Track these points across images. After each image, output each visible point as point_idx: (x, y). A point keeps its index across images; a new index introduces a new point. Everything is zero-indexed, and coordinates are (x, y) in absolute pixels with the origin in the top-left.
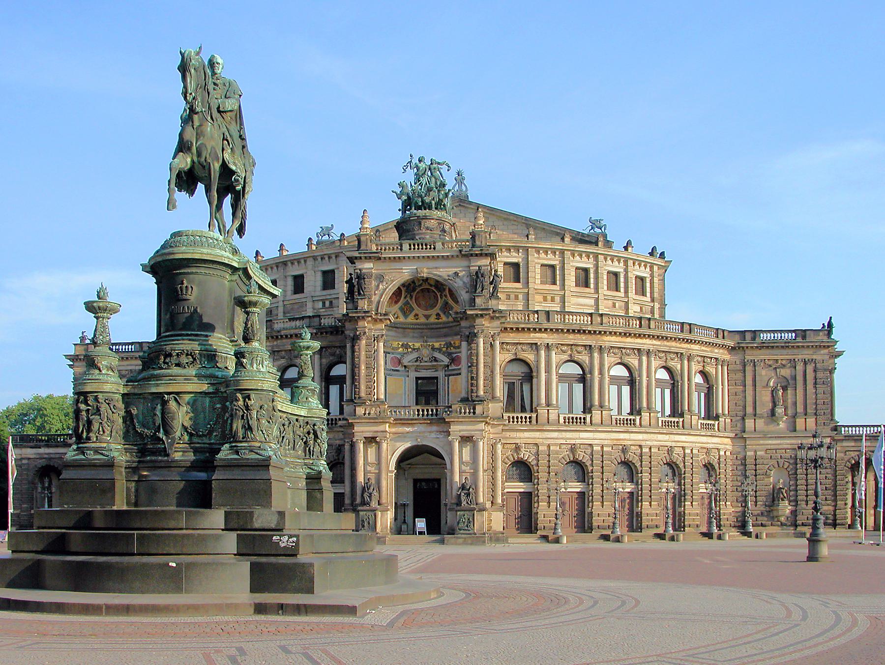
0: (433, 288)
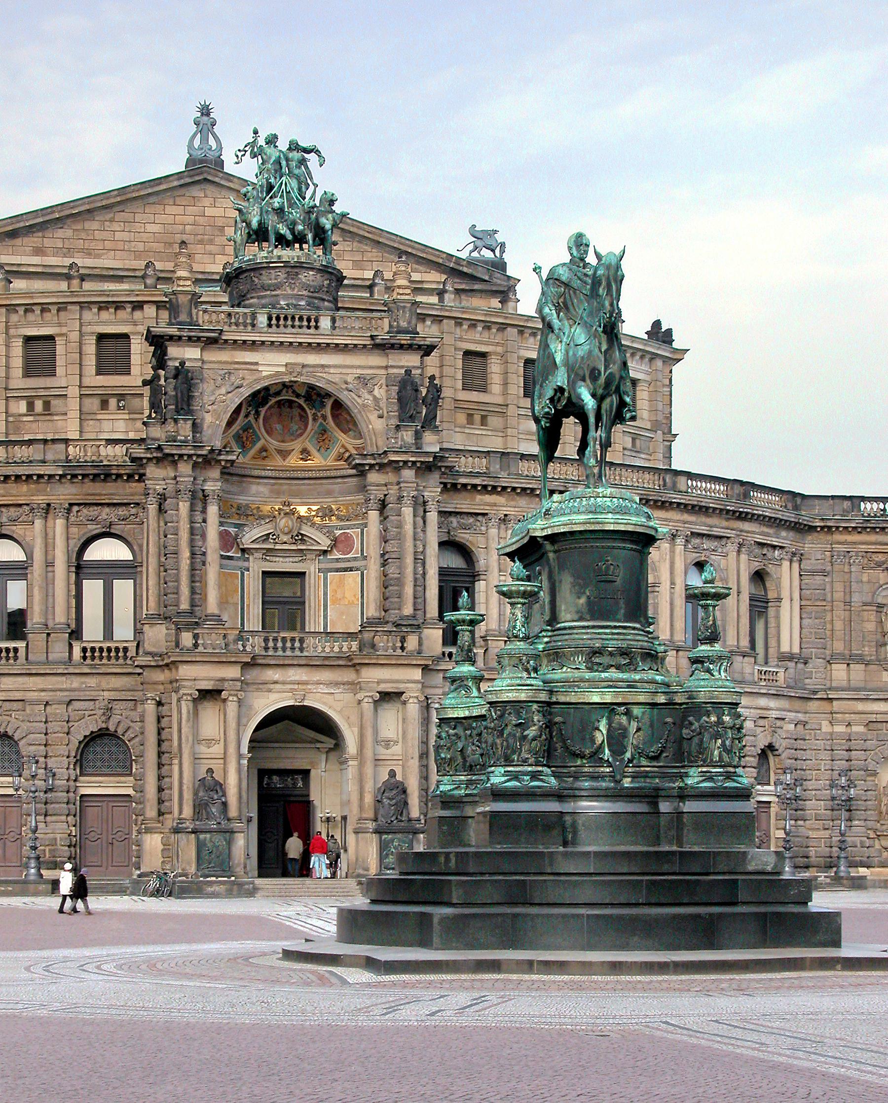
0: (301, 401)
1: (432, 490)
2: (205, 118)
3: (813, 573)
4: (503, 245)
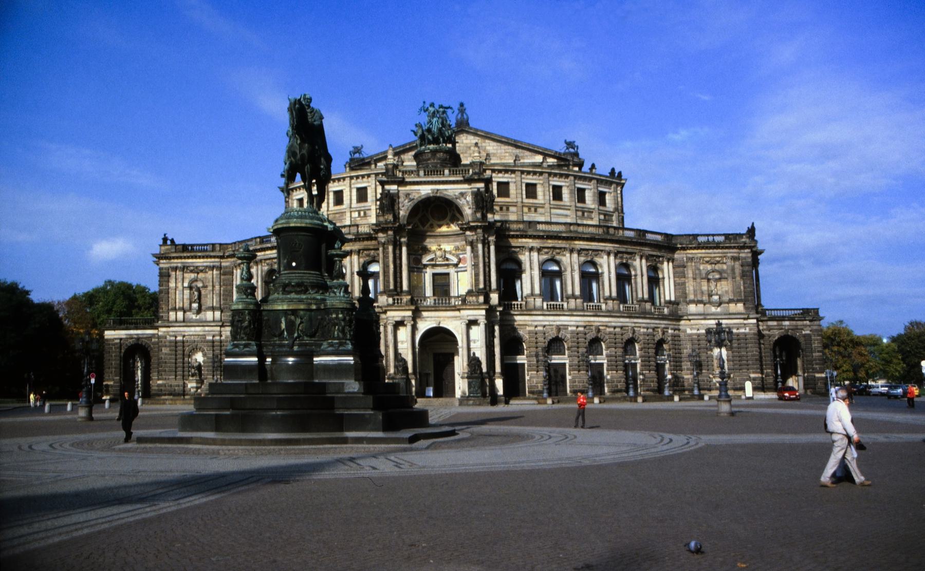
2: (462, 108)
3: (679, 267)
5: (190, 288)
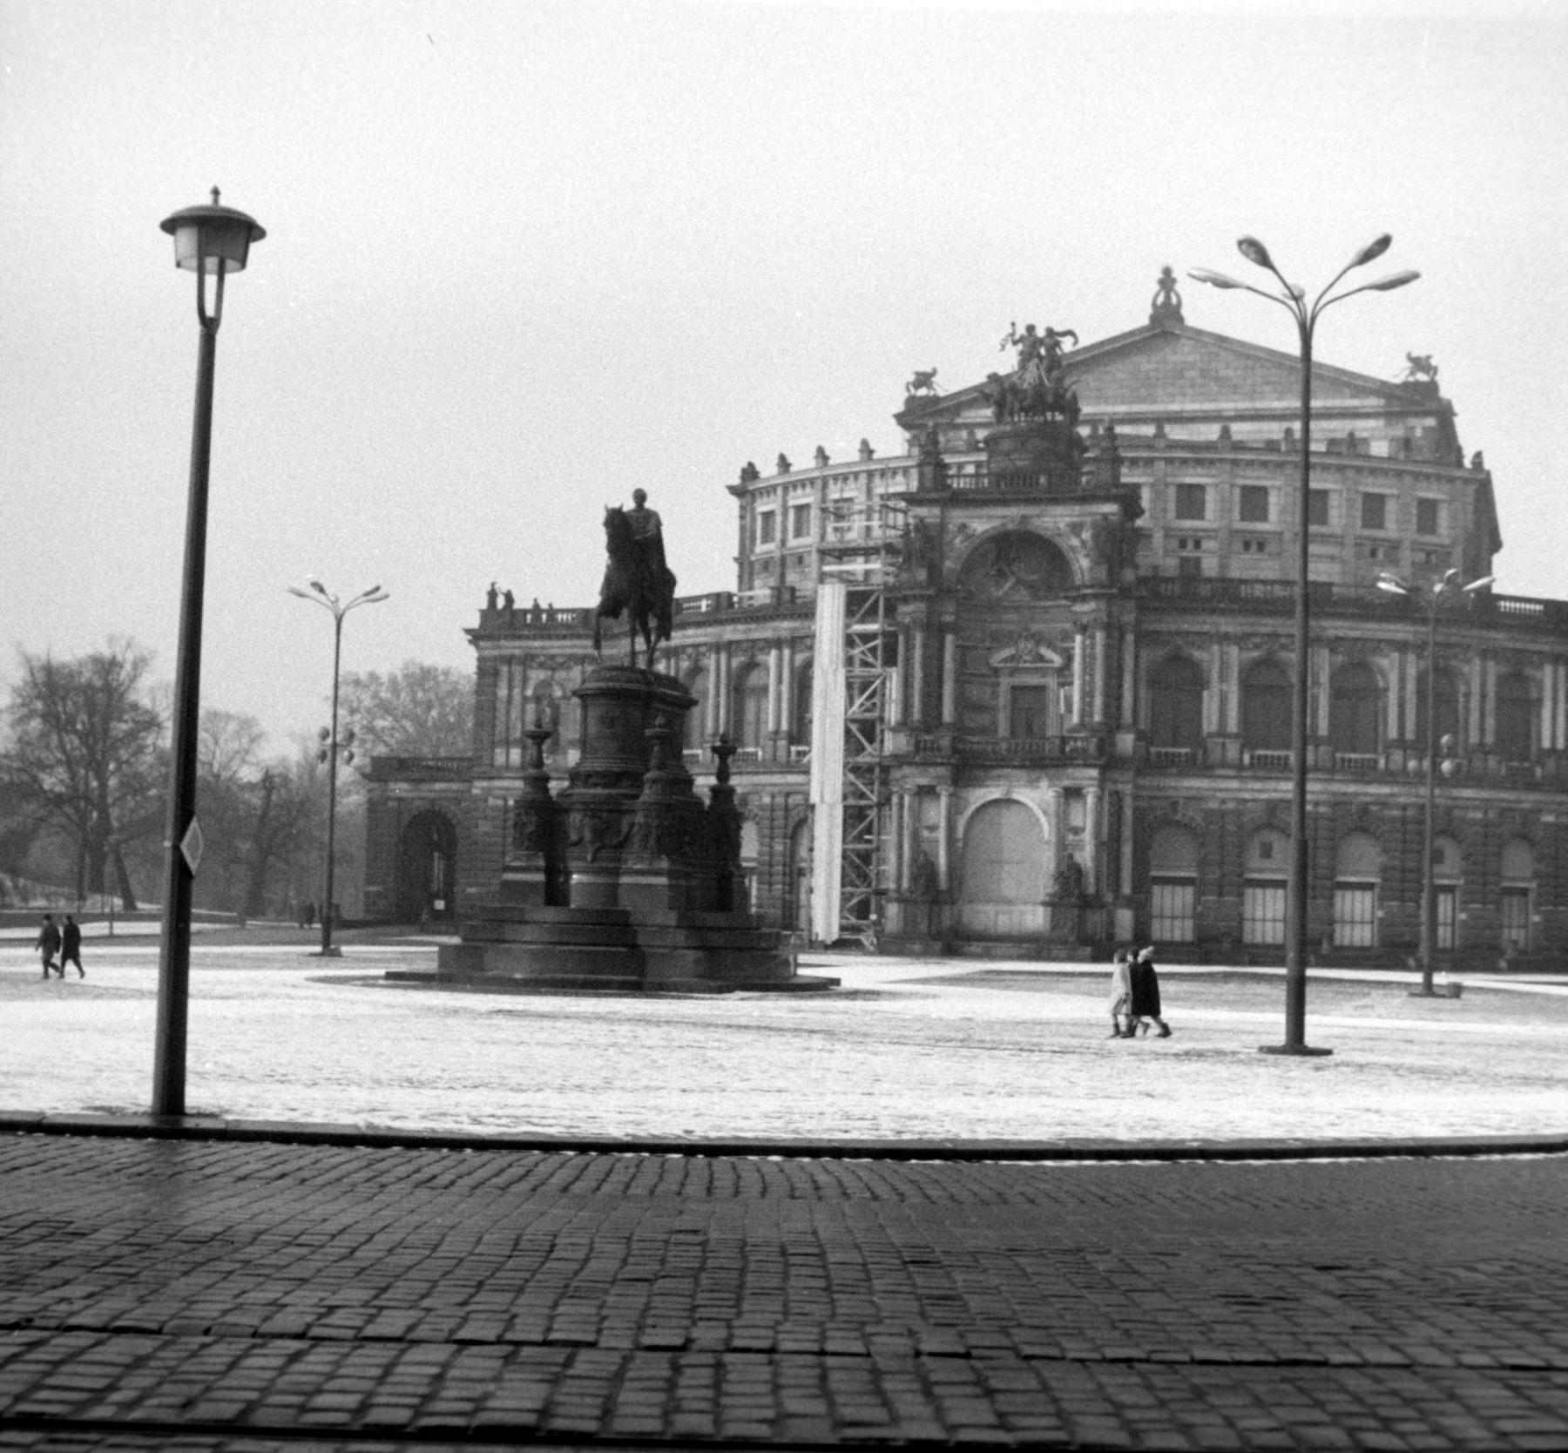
1: (1129, 618)
4: (1435, 370)
5: (538, 699)
